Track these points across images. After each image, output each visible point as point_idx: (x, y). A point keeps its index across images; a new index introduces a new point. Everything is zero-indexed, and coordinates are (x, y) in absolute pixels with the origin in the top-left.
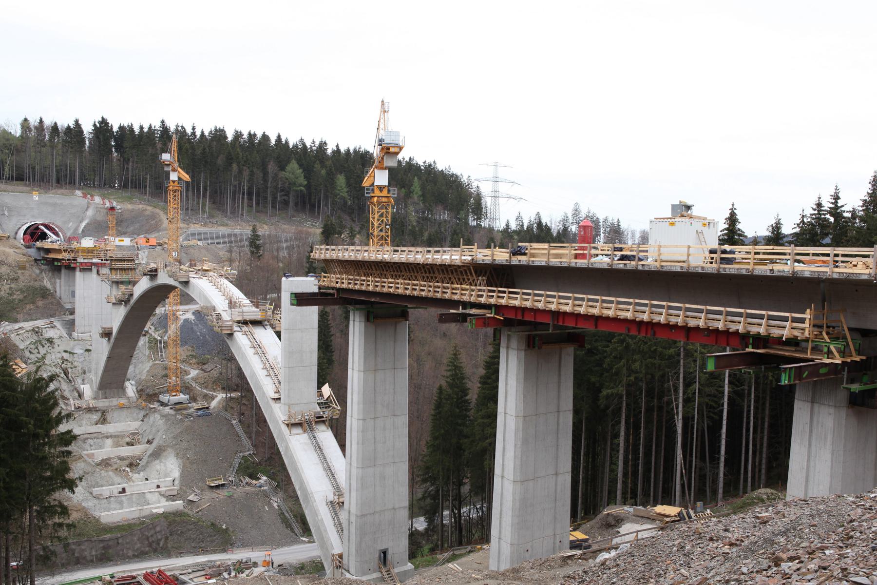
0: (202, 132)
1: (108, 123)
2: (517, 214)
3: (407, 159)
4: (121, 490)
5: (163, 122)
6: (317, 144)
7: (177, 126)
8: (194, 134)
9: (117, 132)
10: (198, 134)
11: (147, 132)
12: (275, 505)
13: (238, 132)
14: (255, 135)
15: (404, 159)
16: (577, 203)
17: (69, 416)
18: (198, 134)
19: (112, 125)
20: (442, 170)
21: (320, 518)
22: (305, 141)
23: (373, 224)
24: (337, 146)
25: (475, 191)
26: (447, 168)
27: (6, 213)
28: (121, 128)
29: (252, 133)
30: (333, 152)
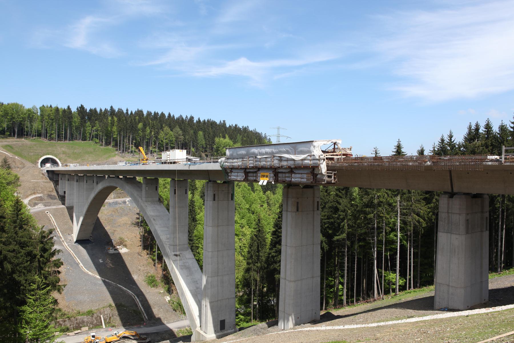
0: (132, 113)
1: (84, 108)
5: (112, 107)
6: (189, 117)
7: (119, 109)
8: (127, 113)
9: (89, 112)
10: (129, 113)
11: (104, 112)
13: (149, 112)
14: (158, 113)
15: (232, 125)
18: (129, 113)
19: (86, 109)
22: (183, 116)
24: (199, 119)
28: (91, 110)
29: (156, 112)
30: (197, 121)
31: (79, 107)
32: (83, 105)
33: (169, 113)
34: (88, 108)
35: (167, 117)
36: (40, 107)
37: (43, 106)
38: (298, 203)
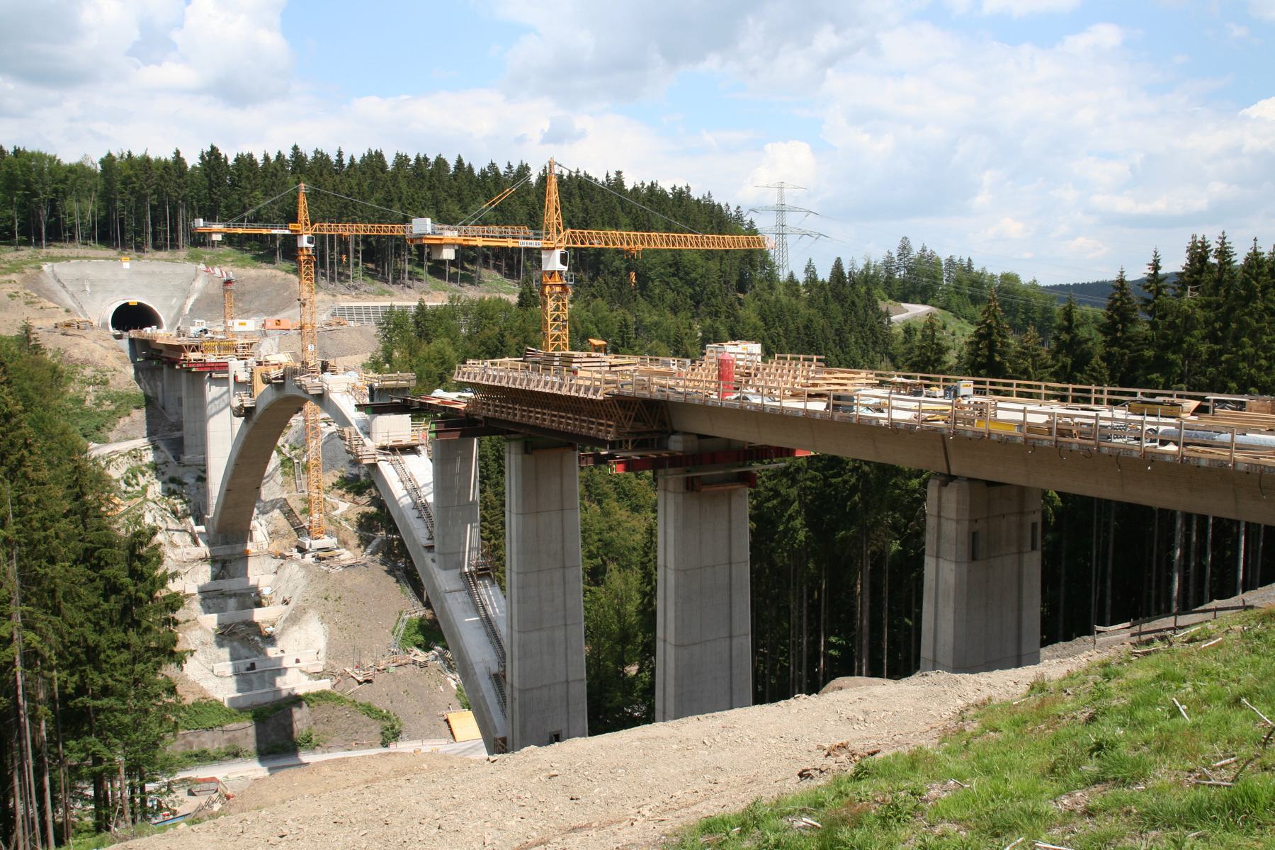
0: (352, 159)
3: (648, 184)
4: (248, 666)
5: (295, 148)
6: (515, 168)
7: (316, 152)
8: (340, 161)
10: (346, 162)
14: (426, 159)
15: (643, 184)
16: (906, 238)
17: (174, 575)
18: (346, 162)
22: (498, 165)
26: (706, 196)
27: (88, 288)
29: (422, 156)
32: (215, 145)
34: (230, 154)
35: (452, 169)
36: (102, 160)
37: (109, 155)
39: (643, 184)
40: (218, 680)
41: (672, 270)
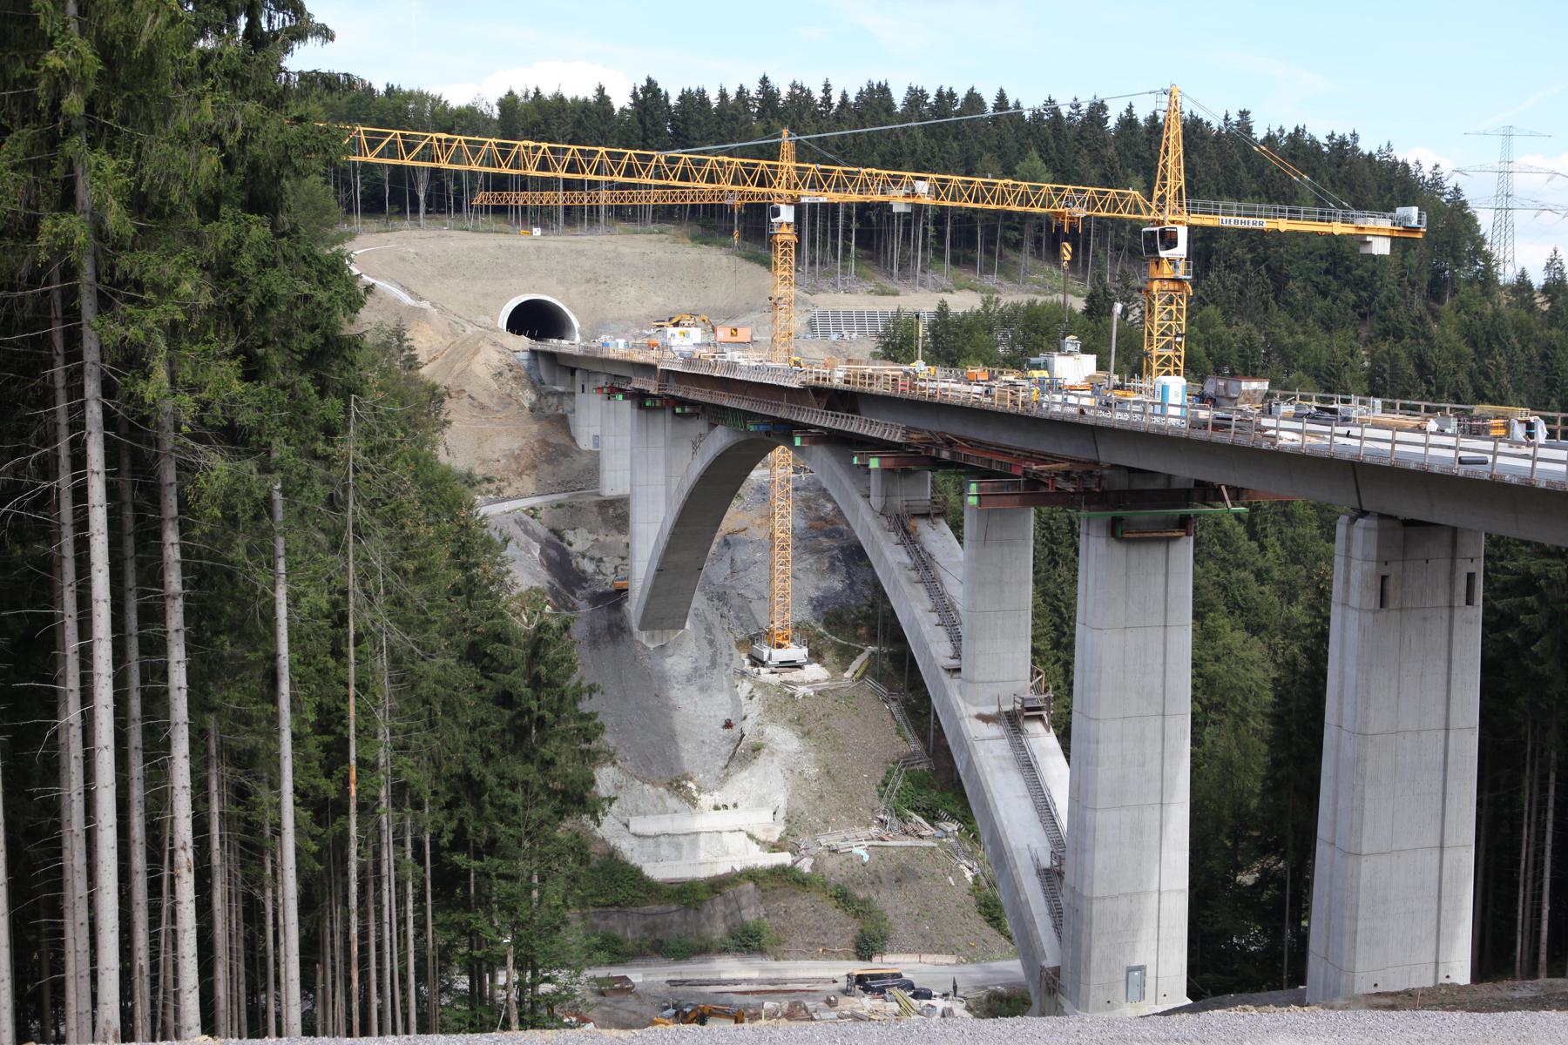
0: (844, 96)
1: (659, 90)
2: (1548, 254)
3: (1290, 130)
5: (764, 81)
6: (1085, 107)
7: (794, 86)
8: (827, 100)
9: (677, 107)
10: (836, 99)
12: (969, 874)
14: (952, 95)
15: (1281, 131)
18: (836, 99)
19: (666, 94)
20: (1370, 154)
21: (1023, 898)
23: (1150, 334)
24: (1129, 111)
25: (1448, 201)
26: (1384, 148)
28: (685, 97)
29: (946, 90)
31: (639, 87)
32: (653, 78)
33: (1001, 90)
37: (511, 93)
38: (1384, 579)
39: (1281, 131)
40: (634, 841)
41: (1324, 265)
